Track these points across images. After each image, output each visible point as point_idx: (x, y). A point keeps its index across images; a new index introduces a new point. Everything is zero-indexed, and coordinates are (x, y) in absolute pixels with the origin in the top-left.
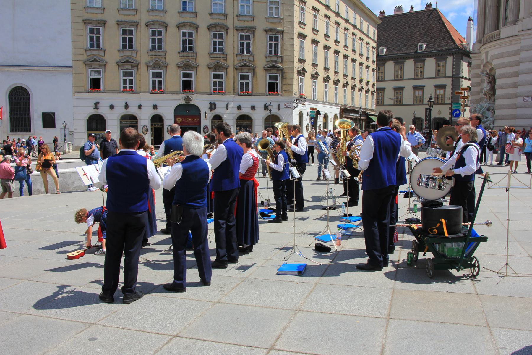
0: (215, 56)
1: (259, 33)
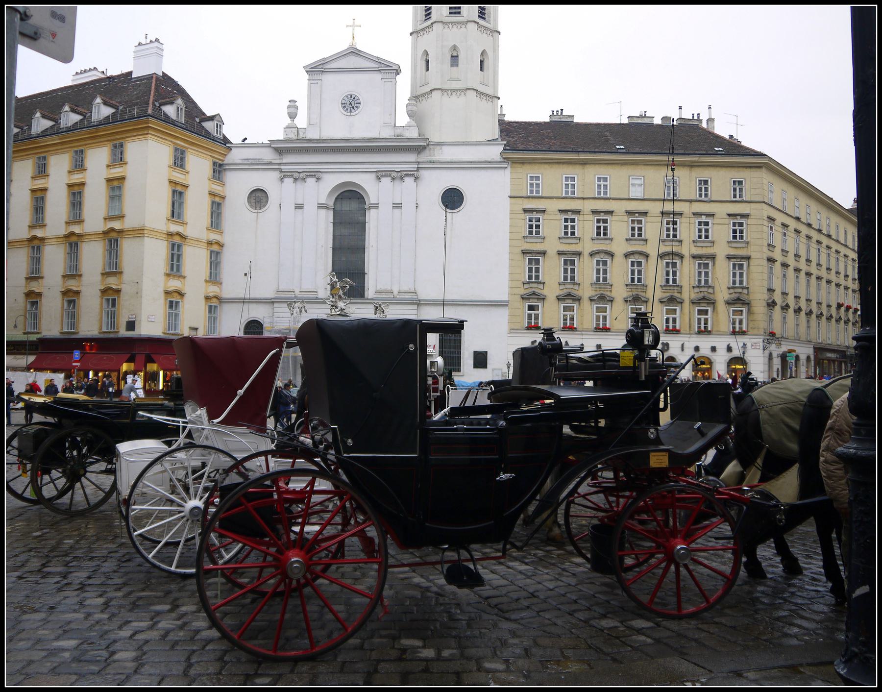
1: (721, 261)
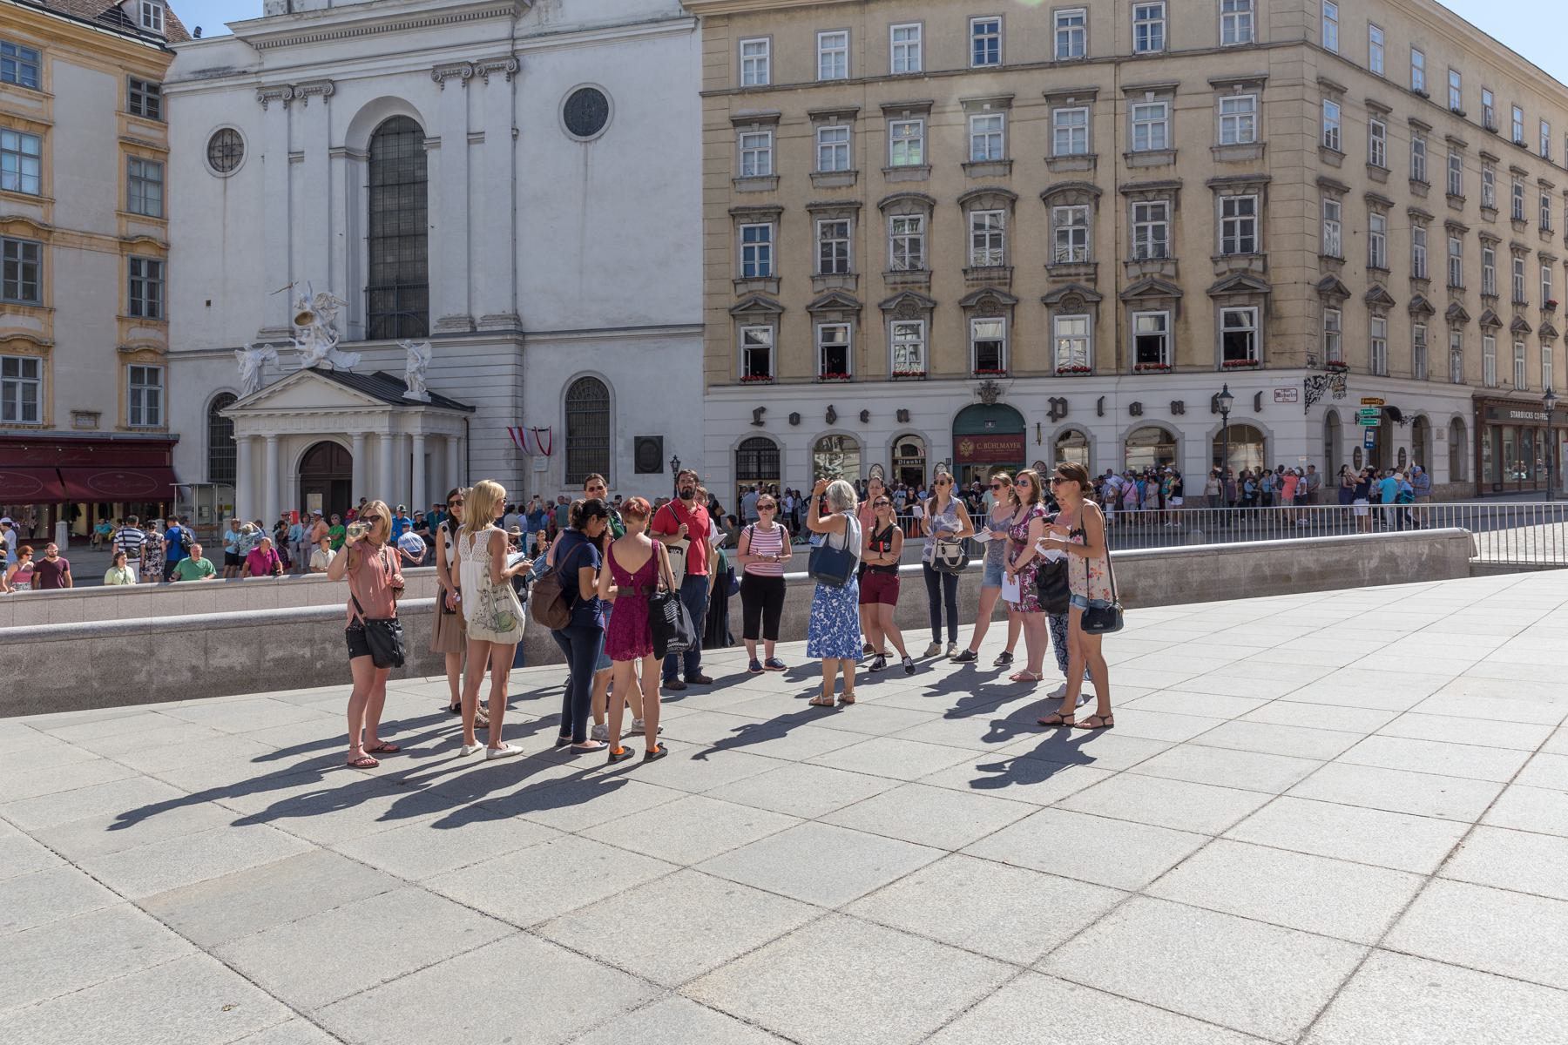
0: (1064, 271)
